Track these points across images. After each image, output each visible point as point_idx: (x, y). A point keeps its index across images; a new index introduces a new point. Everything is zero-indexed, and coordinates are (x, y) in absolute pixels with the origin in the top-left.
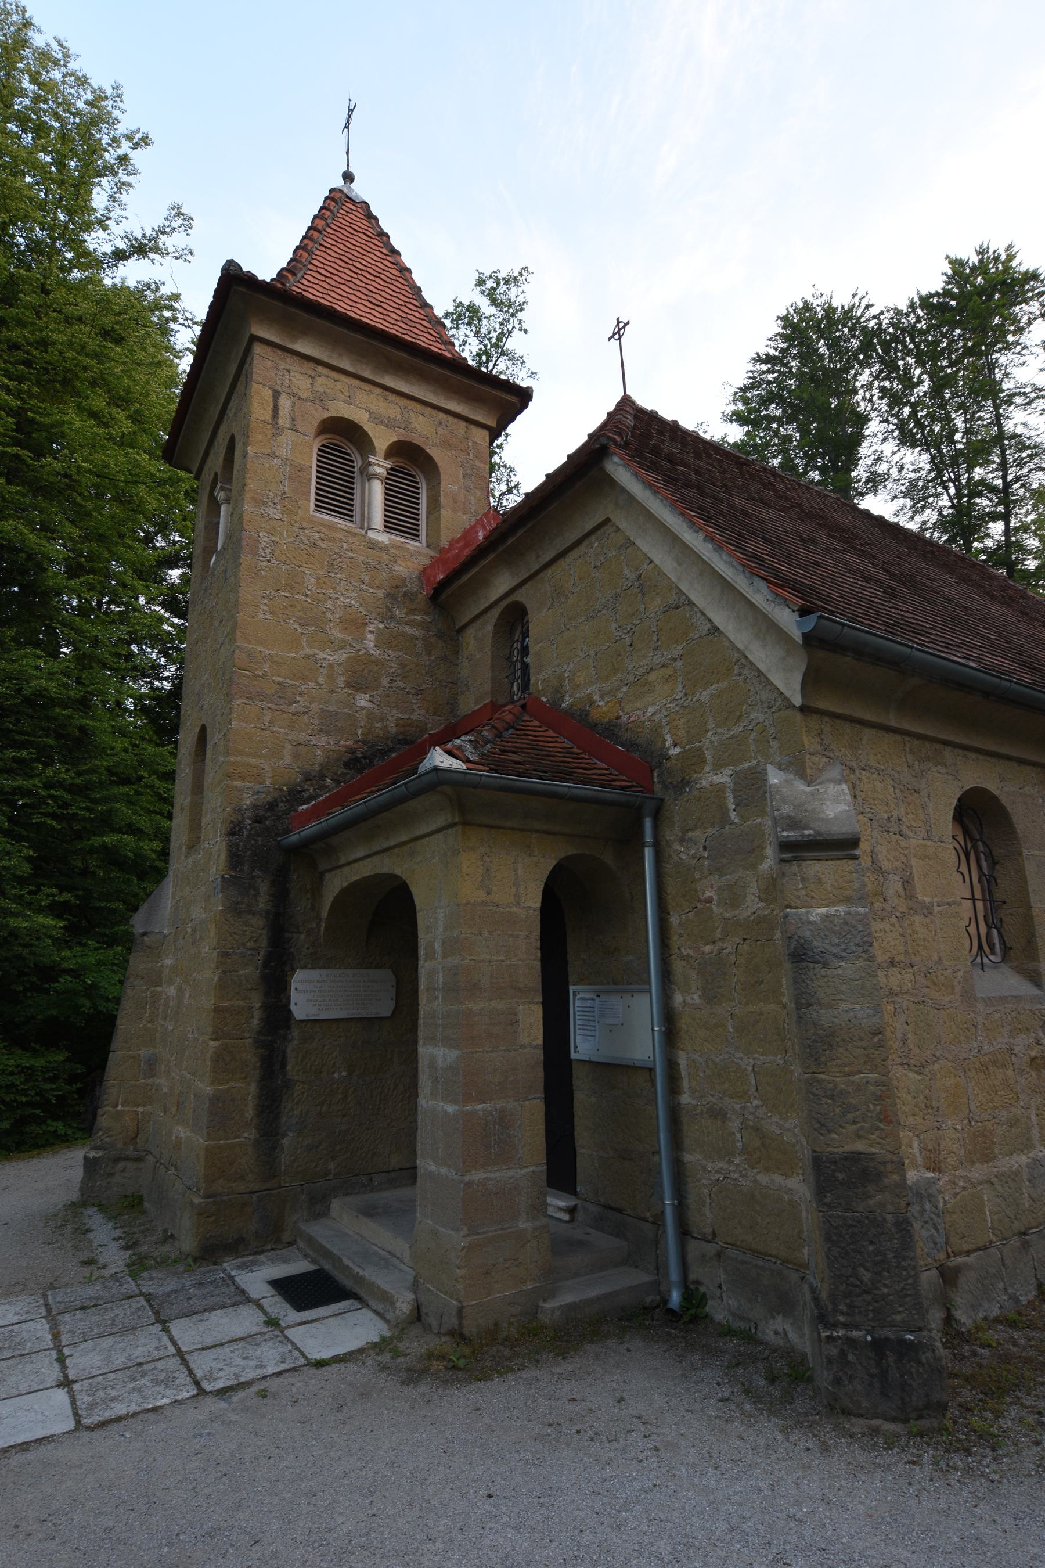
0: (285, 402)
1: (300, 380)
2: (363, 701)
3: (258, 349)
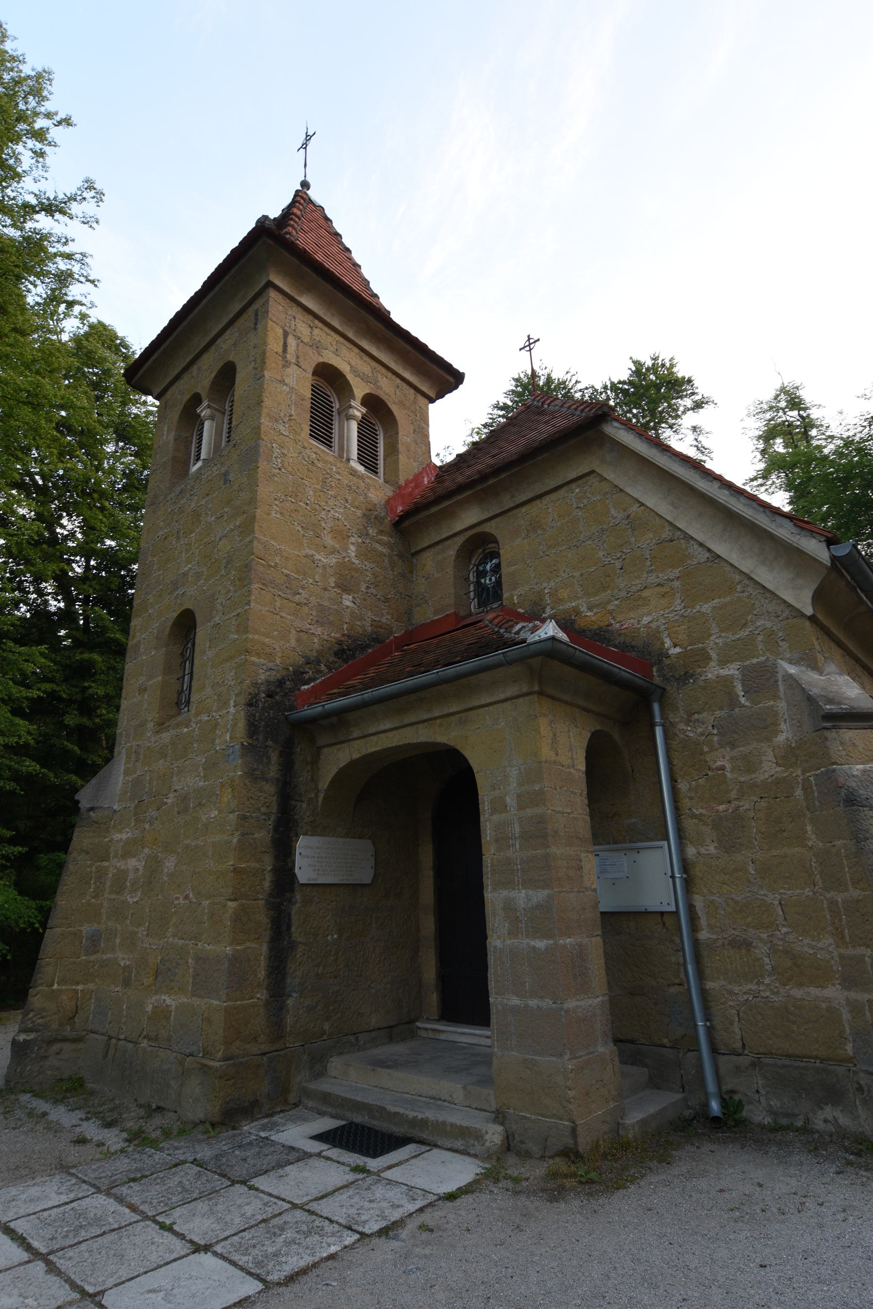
0: (292, 342)
1: (302, 326)
3: (273, 294)
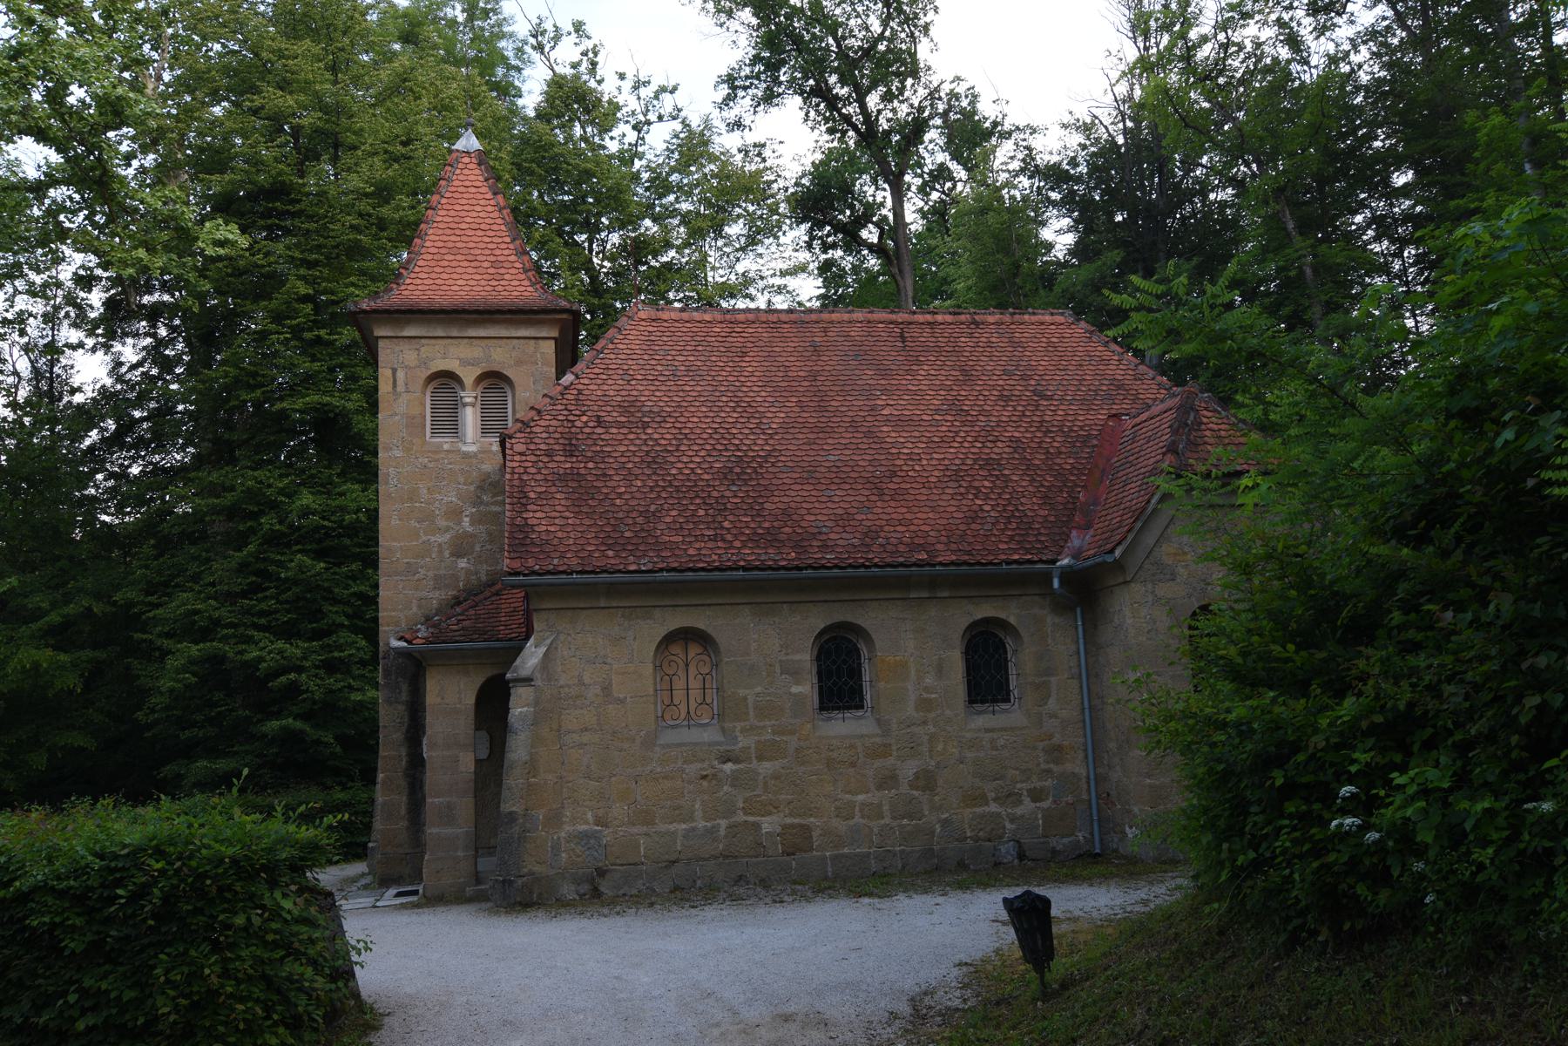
0: (400, 375)
1: (409, 355)
2: (463, 563)
3: (381, 344)
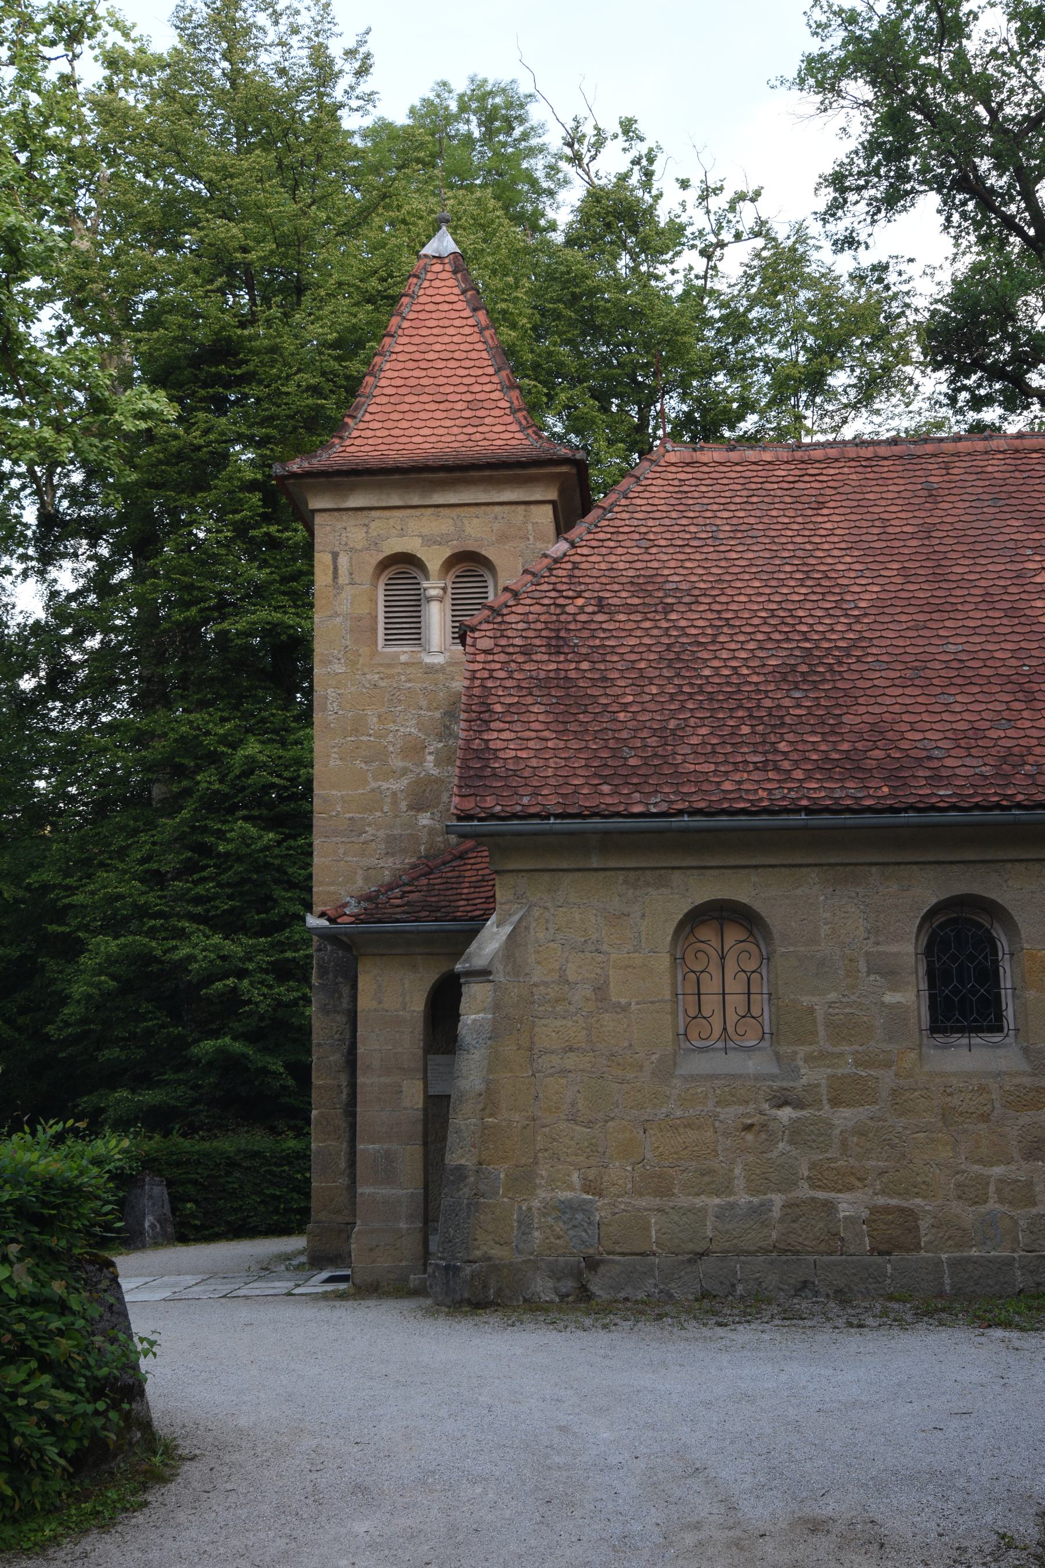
0: (343, 561)
2: (425, 820)
3: (318, 519)
